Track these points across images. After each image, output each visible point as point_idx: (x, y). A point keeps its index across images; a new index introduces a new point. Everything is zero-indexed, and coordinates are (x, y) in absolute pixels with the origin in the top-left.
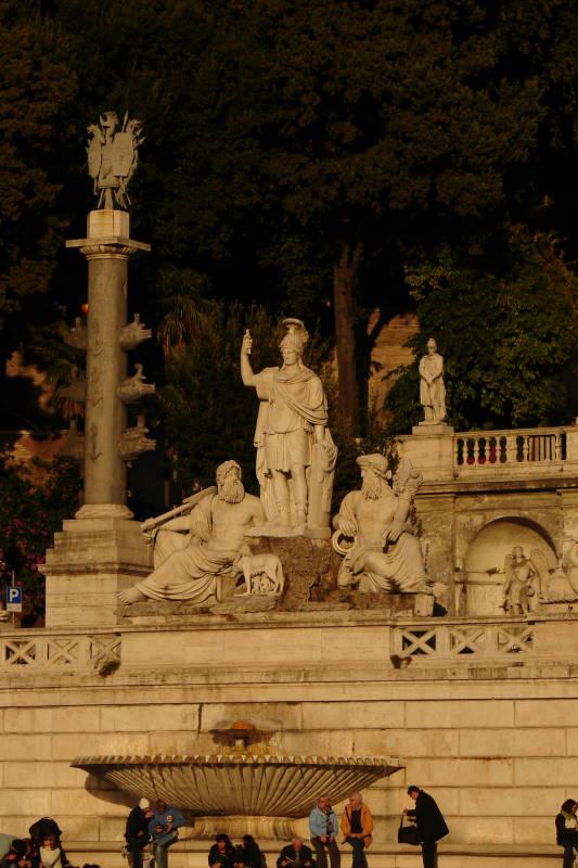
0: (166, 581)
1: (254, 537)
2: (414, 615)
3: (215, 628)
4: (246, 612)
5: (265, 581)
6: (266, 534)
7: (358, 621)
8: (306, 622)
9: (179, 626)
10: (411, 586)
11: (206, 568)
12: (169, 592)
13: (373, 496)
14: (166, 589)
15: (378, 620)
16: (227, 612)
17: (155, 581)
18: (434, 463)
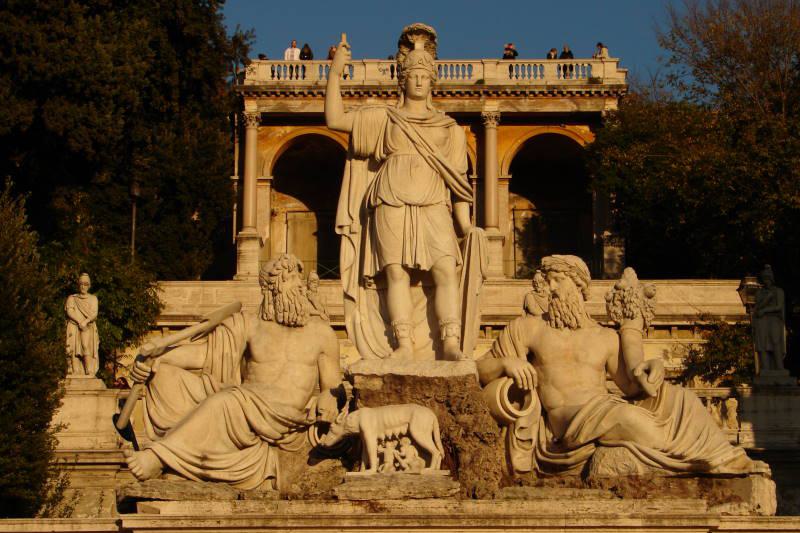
0: (204, 446)
1: (374, 376)
2: (752, 512)
3: (346, 523)
4: (406, 498)
5: (409, 450)
6: (400, 371)
7: (649, 518)
8: (541, 518)
9: (269, 518)
10: (726, 464)
11: (265, 426)
12: (208, 464)
13: (574, 323)
14: (204, 458)
15: (689, 518)
16: (370, 497)
17: (186, 441)
18: (89, 427)
